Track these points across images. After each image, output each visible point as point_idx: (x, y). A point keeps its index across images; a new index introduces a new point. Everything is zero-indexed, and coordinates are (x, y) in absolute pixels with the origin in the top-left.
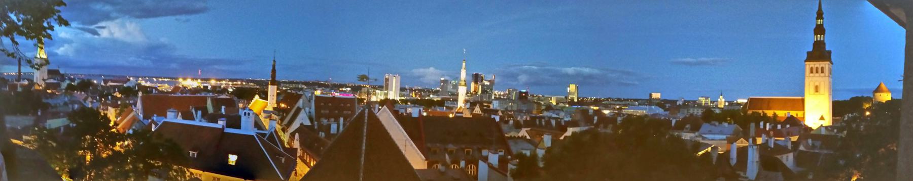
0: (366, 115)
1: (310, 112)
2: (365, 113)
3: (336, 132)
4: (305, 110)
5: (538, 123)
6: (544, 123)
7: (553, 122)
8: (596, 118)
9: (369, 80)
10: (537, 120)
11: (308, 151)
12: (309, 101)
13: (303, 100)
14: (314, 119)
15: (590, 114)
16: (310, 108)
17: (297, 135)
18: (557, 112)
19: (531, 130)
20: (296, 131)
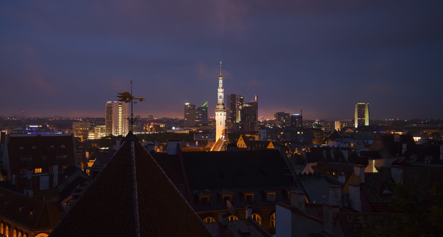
5: (325, 155)
6: (333, 156)
7: (346, 154)
9: (133, 100)
10: (324, 152)
11: (6, 221)
15: (396, 140)
19: (318, 165)
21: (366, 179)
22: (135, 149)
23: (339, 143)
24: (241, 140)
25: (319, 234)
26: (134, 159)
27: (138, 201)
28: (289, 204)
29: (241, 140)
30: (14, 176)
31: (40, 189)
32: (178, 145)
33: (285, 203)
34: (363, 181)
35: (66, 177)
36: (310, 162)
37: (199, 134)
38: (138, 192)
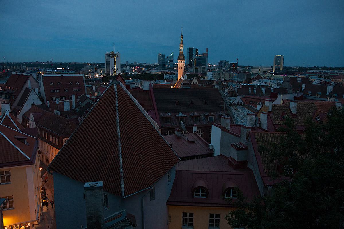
0: (116, 90)
1: (39, 92)
2: (114, 89)
3: (69, 110)
4: (34, 90)
5: (250, 91)
6: (255, 91)
7: (264, 90)
8: (304, 86)
10: (250, 88)
12: (38, 82)
13: (31, 81)
14: (45, 99)
16: (40, 89)
17: (31, 116)
18: (265, 80)
19: (244, 97)
20: (29, 111)
21: (272, 109)
22: (117, 89)
23: (260, 82)
24: (195, 79)
25: (237, 144)
26: (116, 96)
27: (119, 123)
28: (220, 124)
29: (195, 79)
30: (48, 102)
31: (65, 110)
32: (150, 83)
33: (217, 124)
34: (271, 110)
35: (80, 103)
36: (239, 95)
37: (167, 75)
38: (119, 117)
